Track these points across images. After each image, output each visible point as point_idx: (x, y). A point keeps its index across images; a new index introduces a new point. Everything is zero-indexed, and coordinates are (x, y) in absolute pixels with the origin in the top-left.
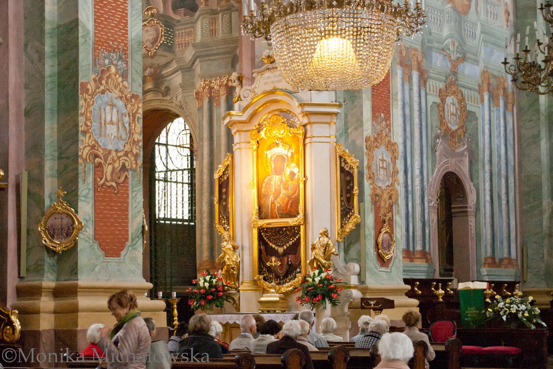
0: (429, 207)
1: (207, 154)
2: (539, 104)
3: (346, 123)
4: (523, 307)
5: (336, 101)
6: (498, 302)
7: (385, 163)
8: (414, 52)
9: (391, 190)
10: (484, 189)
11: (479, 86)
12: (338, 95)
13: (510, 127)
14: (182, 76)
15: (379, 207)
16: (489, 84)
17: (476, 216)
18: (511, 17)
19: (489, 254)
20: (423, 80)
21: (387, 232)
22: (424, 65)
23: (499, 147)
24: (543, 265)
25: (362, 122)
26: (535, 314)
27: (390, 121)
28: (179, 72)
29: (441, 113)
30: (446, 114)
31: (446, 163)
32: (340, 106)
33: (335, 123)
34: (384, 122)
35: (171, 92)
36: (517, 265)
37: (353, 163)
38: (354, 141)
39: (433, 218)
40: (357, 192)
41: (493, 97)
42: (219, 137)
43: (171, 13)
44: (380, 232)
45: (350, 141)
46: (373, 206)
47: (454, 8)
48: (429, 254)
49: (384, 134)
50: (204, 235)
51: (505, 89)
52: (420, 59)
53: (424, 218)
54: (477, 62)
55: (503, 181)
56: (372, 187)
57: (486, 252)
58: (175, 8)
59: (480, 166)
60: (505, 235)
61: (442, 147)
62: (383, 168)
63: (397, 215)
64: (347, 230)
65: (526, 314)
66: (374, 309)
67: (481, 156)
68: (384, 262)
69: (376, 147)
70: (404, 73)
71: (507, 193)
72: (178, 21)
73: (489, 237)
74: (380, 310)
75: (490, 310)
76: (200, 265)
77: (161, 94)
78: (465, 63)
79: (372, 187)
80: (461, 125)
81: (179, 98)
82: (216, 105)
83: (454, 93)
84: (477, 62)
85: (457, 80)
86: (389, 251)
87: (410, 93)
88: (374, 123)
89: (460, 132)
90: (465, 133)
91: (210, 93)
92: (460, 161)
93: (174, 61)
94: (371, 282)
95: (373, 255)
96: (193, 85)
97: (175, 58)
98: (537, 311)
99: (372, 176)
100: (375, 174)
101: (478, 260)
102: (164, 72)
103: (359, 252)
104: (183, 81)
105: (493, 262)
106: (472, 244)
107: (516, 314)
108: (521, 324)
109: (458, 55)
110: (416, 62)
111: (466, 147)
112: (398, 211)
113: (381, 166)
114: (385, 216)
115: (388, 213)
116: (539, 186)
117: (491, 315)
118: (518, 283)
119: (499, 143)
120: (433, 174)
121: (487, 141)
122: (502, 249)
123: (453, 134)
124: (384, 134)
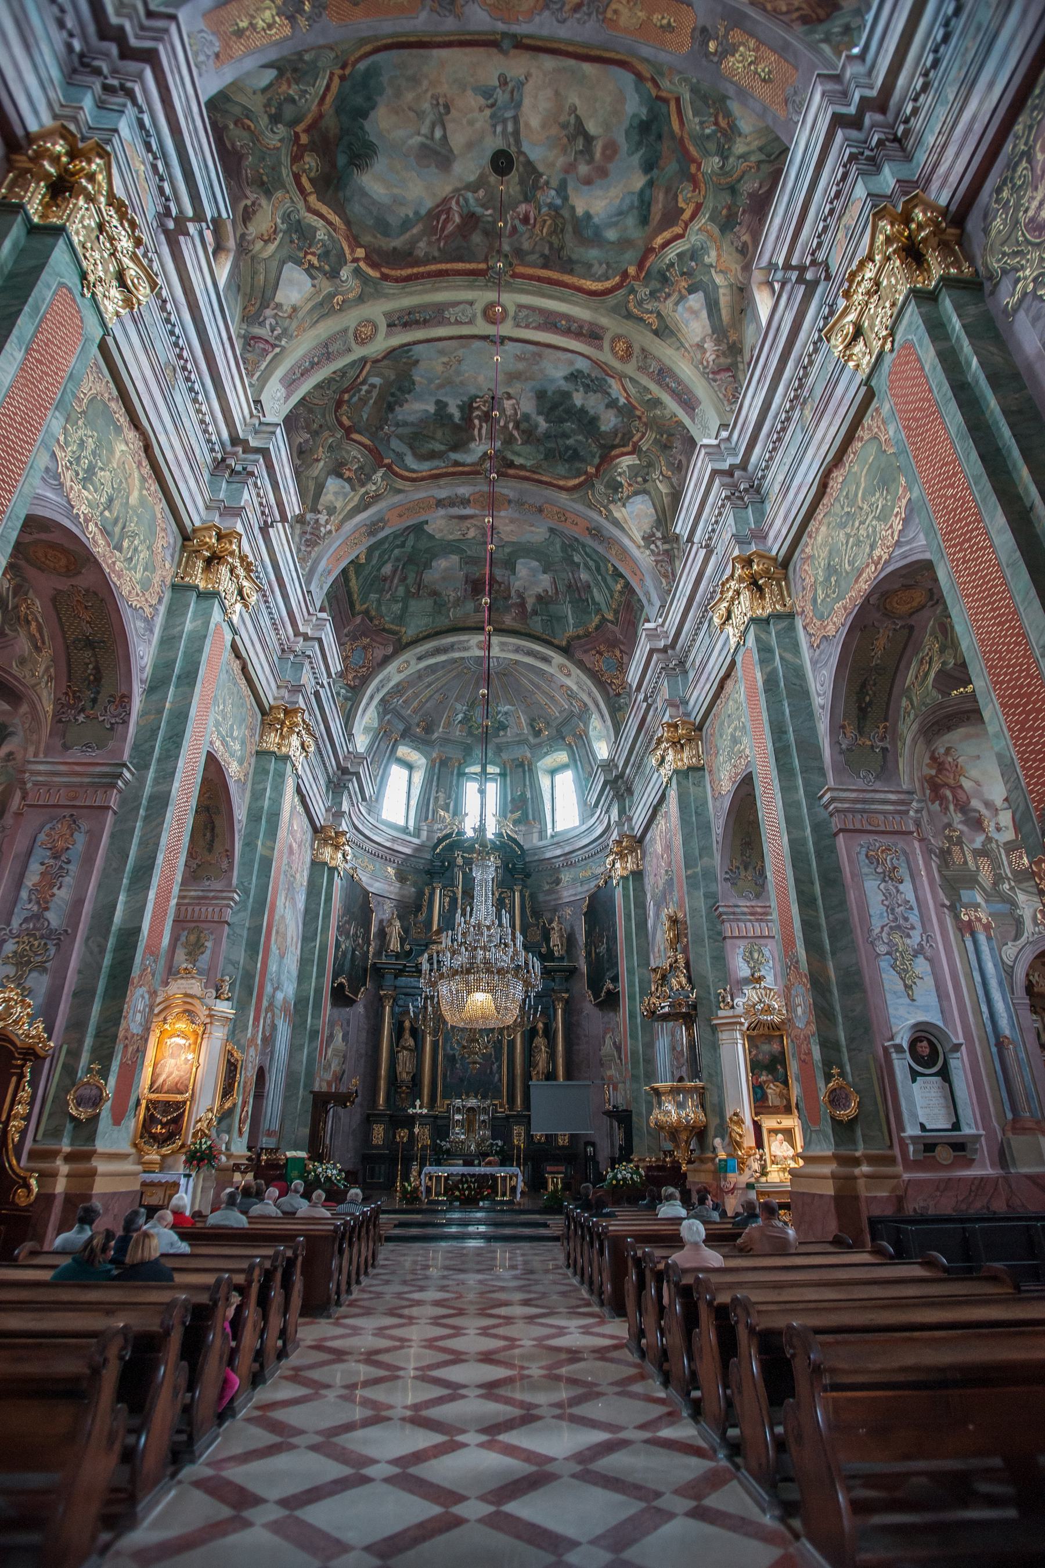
119: (283, 1047)
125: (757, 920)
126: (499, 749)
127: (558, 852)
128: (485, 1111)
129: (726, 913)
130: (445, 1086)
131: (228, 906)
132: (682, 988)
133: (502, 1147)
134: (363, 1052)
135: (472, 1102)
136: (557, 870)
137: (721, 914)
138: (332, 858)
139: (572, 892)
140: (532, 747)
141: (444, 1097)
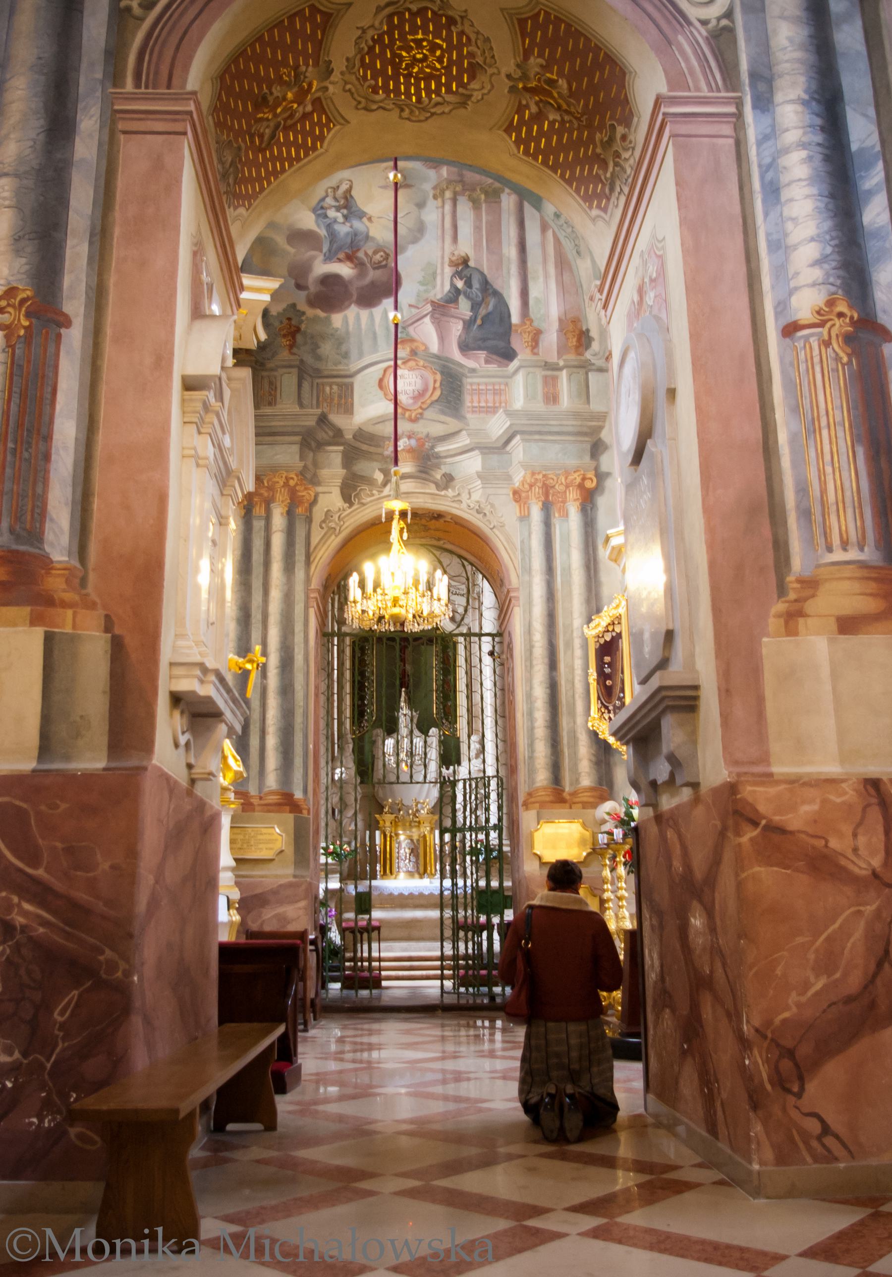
1: (542, 596)
14: (482, 458)
28: (477, 452)
35: (457, 484)
42: (567, 570)
43: (456, 355)
50: (537, 741)
58: (465, 347)
72: (473, 370)
76: (530, 795)
77: (433, 486)
81: (477, 496)
82: (560, 516)
91: (547, 495)
93: (464, 432)
96: (509, 478)
97: (467, 428)
102: (440, 449)
104: (483, 468)
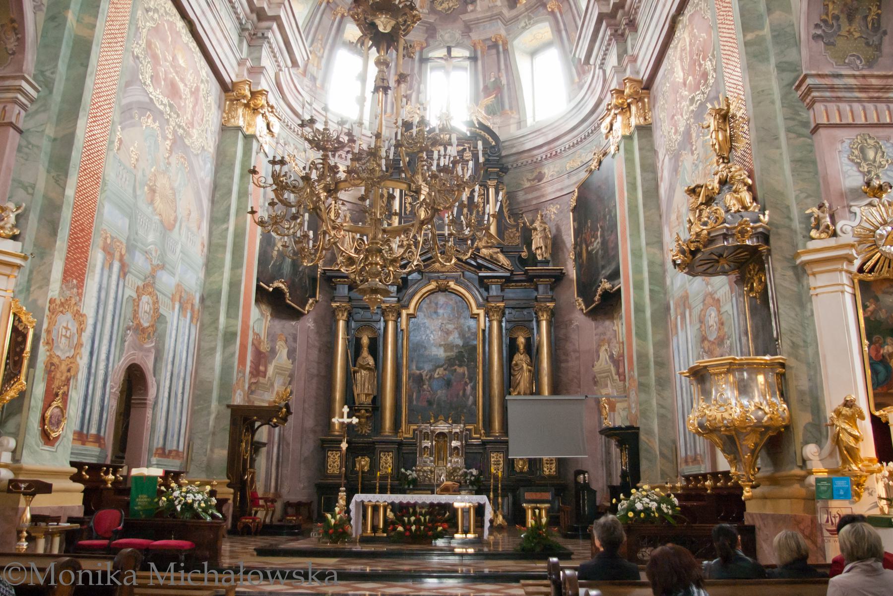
0: (110, 392)
2: (218, 323)
3: (29, 281)
4: (199, 497)
5: (22, 252)
6: (173, 491)
7: (69, 332)
8: (118, 244)
9: (71, 363)
10: (164, 387)
11: (173, 295)
12: (25, 247)
13: (192, 337)
15: (54, 378)
16: (181, 297)
17: (154, 409)
18: (205, 250)
19: (161, 444)
20: (124, 271)
21: (57, 407)
22: (126, 258)
23: (181, 352)
24: (205, 459)
25: (49, 281)
26: (211, 505)
27: (82, 290)
29: (136, 308)
30: (140, 310)
31: (133, 354)
32: (25, 258)
33: (16, 277)
34: (75, 289)
36: (183, 458)
37: (29, 322)
38: (35, 301)
39: (112, 404)
40: (29, 355)
41: (182, 308)
44: (50, 406)
45: (30, 299)
46: (46, 375)
47: (161, 222)
48: (104, 439)
49: (73, 302)
51: (192, 305)
52: (123, 252)
53: (104, 403)
54: (173, 274)
55: (181, 382)
56: (48, 353)
57: (158, 443)
59: (164, 364)
60: (176, 430)
61: (131, 339)
62: (65, 336)
63: (74, 390)
64: (7, 398)
65: (203, 505)
66: (25, 494)
67: (165, 356)
68: (49, 439)
69: (62, 312)
70: (105, 259)
71: (183, 393)
73: (163, 430)
74: (33, 494)
75: (164, 499)
78: (164, 272)
79: (48, 353)
80: (152, 323)
83: (150, 294)
84: (173, 274)
85: (154, 283)
86: (58, 427)
87: (108, 280)
88: (64, 286)
89: (150, 330)
90: (154, 332)
92: (147, 356)
94: (28, 461)
95: (36, 431)
98: (214, 501)
99: (50, 341)
100: (55, 341)
101: (150, 450)
103: (18, 426)
105: (163, 453)
106: (146, 435)
107: (191, 505)
108: (197, 516)
109: (159, 262)
110: (119, 254)
111: (153, 344)
112: (76, 386)
113: (64, 334)
114: (59, 388)
115: (64, 386)
116: (210, 391)
117: (165, 504)
118: (183, 473)
119: (182, 348)
120: (119, 362)
121: (172, 345)
122: (172, 441)
123: (143, 330)
124: (73, 302)
125: (871, 100)
126: (468, 29)
127: (540, 141)
128: (457, 436)
129: (818, 88)
130: (411, 410)
131: (15, 101)
132: (745, 208)
133: (477, 478)
134: (315, 371)
135: (442, 427)
136: (538, 164)
137: (810, 89)
138: (249, 125)
139: (558, 186)
140: (507, 22)
141: (410, 422)
